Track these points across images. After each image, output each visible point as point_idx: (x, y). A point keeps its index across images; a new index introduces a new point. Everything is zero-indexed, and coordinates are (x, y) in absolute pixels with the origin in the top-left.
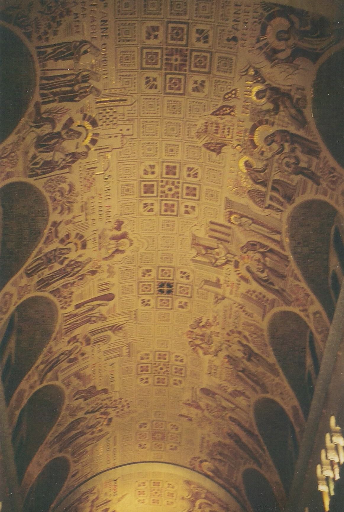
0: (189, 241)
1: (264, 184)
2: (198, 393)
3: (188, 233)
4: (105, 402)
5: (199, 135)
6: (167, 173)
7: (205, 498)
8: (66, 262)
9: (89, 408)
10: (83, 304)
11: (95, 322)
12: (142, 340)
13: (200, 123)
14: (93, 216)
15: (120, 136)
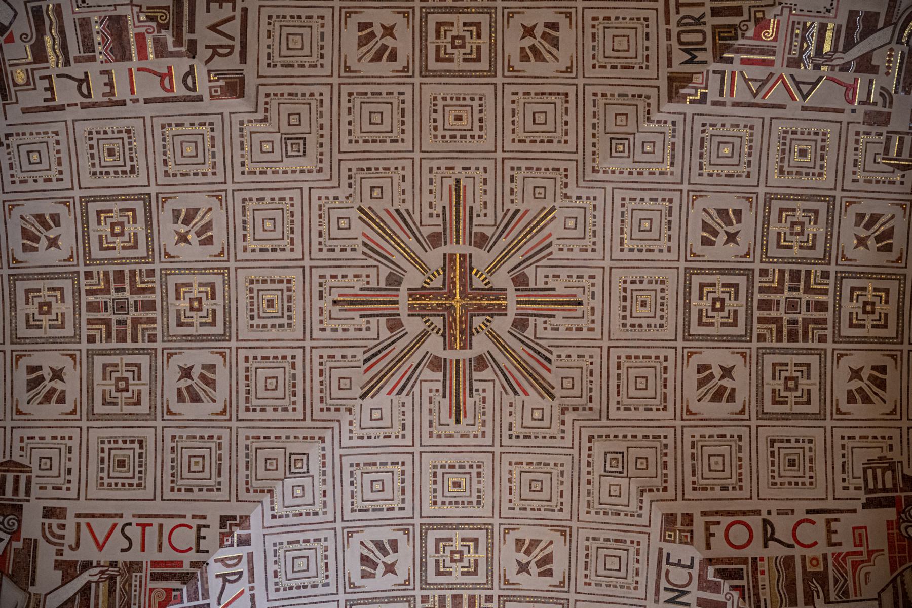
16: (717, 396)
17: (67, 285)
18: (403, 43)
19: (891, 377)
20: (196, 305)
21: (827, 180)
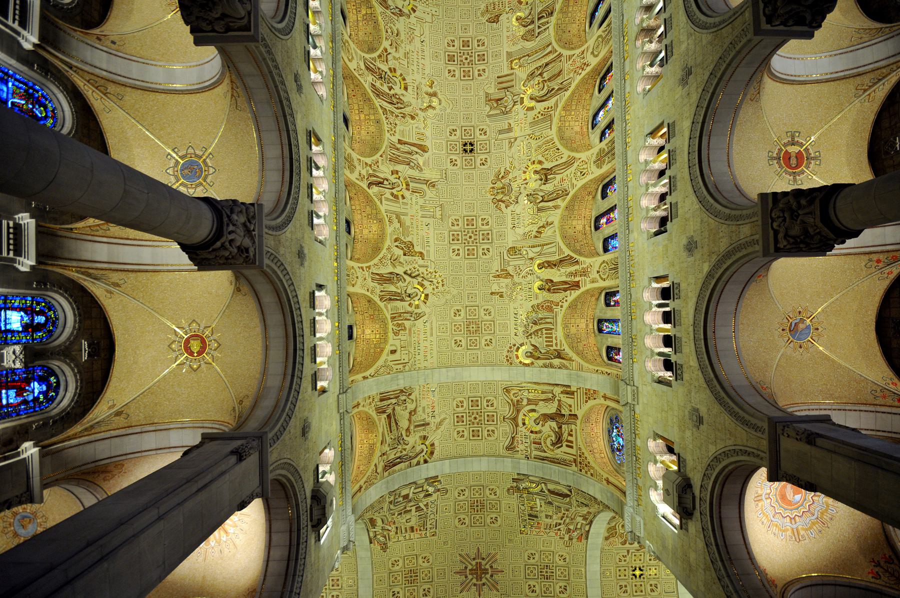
0: (483, 100)
1: (533, 22)
2: (506, 257)
3: (482, 93)
4: (422, 270)
5: (483, 15)
6: (463, 46)
7: (528, 404)
8: (392, 92)
9: (407, 268)
10: (405, 143)
11: (412, 168)
12: (452, 203)
13: (483, 7)
14: (412, 67)
15: (430, 14)
16: (533, 592)
17: (400, 573)
18: (467, 521)
19: (568, 588)
20: (426, 575)
21: (552, 548)
